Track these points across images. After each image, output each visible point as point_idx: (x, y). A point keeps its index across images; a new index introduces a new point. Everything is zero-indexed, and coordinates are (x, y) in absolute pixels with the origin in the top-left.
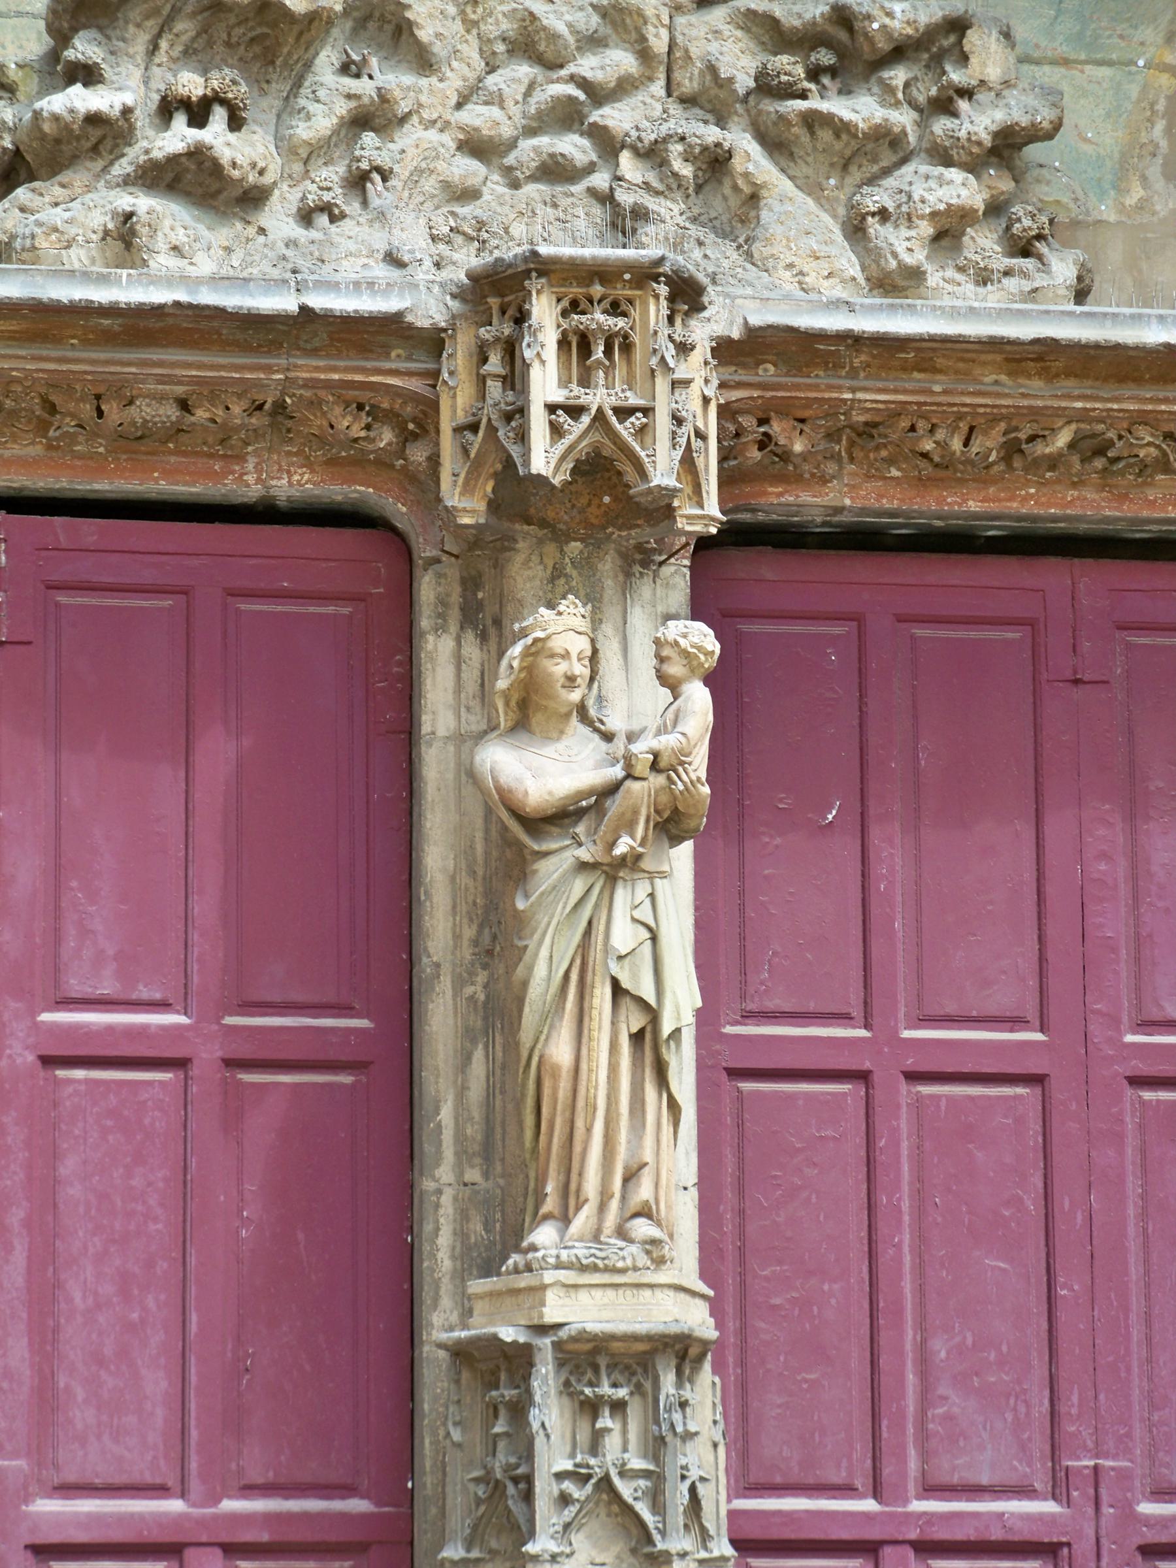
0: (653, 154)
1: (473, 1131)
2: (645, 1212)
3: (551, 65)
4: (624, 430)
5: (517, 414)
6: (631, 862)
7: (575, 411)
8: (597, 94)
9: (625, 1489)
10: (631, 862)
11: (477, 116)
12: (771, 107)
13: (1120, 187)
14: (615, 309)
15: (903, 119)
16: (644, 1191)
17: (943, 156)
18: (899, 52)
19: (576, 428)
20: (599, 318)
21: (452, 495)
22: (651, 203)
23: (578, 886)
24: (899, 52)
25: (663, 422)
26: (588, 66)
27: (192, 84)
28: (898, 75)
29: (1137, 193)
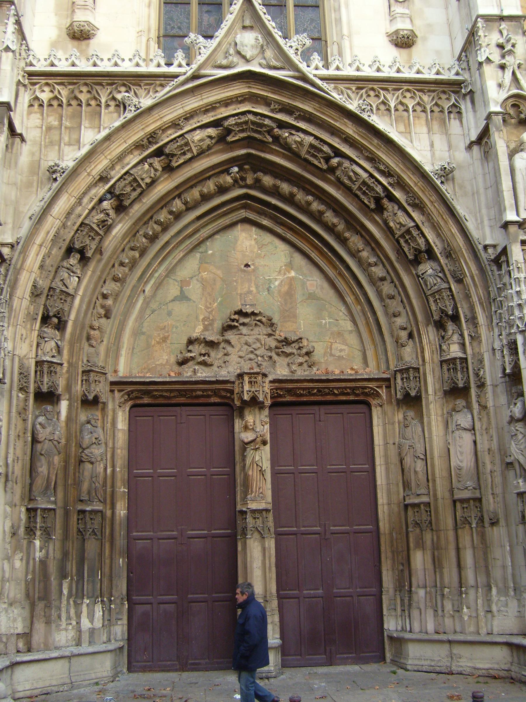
0: (262, 357)
1: (242, 483)
2: (262, 493)
3: (250, 346)
4: (256, 393)
5: (243, 392)
6: (258, 448)
7: (250, 391)
8: (255, 350)
9: (259, 529)
10: (258, 448)
11: (241, 354)
12: (277, 350)
13: (324, 357)
14: (255, 378)
15: (295, 351)
16: (261, 490)
17: (299, 355)
18: (293, 342)
19: (250, 393)
20: (253, 379)
21: (236, 402)
22: (262, 363)
23: (252, 452)
24: (293, 342)
25: (261, 392)
26: (254, 346)
27: (203, 352)
28: (293, 345)
29: (326, 358)
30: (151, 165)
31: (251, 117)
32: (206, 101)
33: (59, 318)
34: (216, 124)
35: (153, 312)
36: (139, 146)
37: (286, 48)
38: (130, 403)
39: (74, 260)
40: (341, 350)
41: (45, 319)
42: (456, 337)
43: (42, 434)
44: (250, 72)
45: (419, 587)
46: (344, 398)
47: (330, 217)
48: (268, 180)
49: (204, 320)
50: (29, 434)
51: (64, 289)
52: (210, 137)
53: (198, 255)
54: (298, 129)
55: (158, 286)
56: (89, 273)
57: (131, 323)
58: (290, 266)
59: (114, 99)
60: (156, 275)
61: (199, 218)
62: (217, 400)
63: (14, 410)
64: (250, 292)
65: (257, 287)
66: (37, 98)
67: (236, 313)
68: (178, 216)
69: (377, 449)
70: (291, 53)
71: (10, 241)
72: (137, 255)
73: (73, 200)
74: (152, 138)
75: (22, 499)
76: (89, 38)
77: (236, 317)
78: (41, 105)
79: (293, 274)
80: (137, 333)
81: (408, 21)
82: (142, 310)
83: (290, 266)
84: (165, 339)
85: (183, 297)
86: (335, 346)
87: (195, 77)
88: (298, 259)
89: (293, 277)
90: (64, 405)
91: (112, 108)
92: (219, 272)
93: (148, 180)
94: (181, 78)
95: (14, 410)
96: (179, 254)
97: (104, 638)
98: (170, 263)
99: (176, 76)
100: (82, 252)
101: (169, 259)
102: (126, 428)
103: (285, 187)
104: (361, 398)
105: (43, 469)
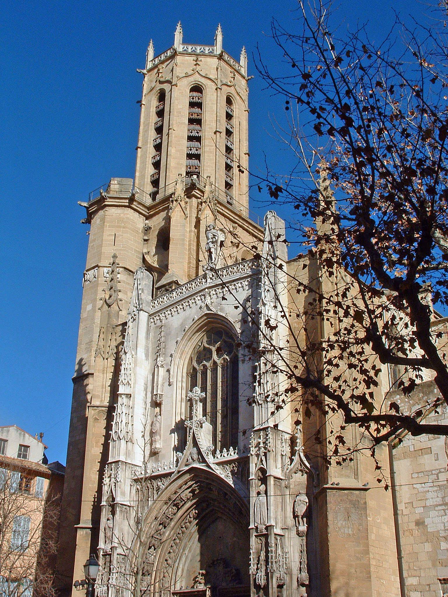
32: (185, 480)
36: (166, 503)
39: (152, 550)
66: (138, 489)
74: (170, 499)
76: (158, 453)
87: (179, 472)
100: (154, 546)
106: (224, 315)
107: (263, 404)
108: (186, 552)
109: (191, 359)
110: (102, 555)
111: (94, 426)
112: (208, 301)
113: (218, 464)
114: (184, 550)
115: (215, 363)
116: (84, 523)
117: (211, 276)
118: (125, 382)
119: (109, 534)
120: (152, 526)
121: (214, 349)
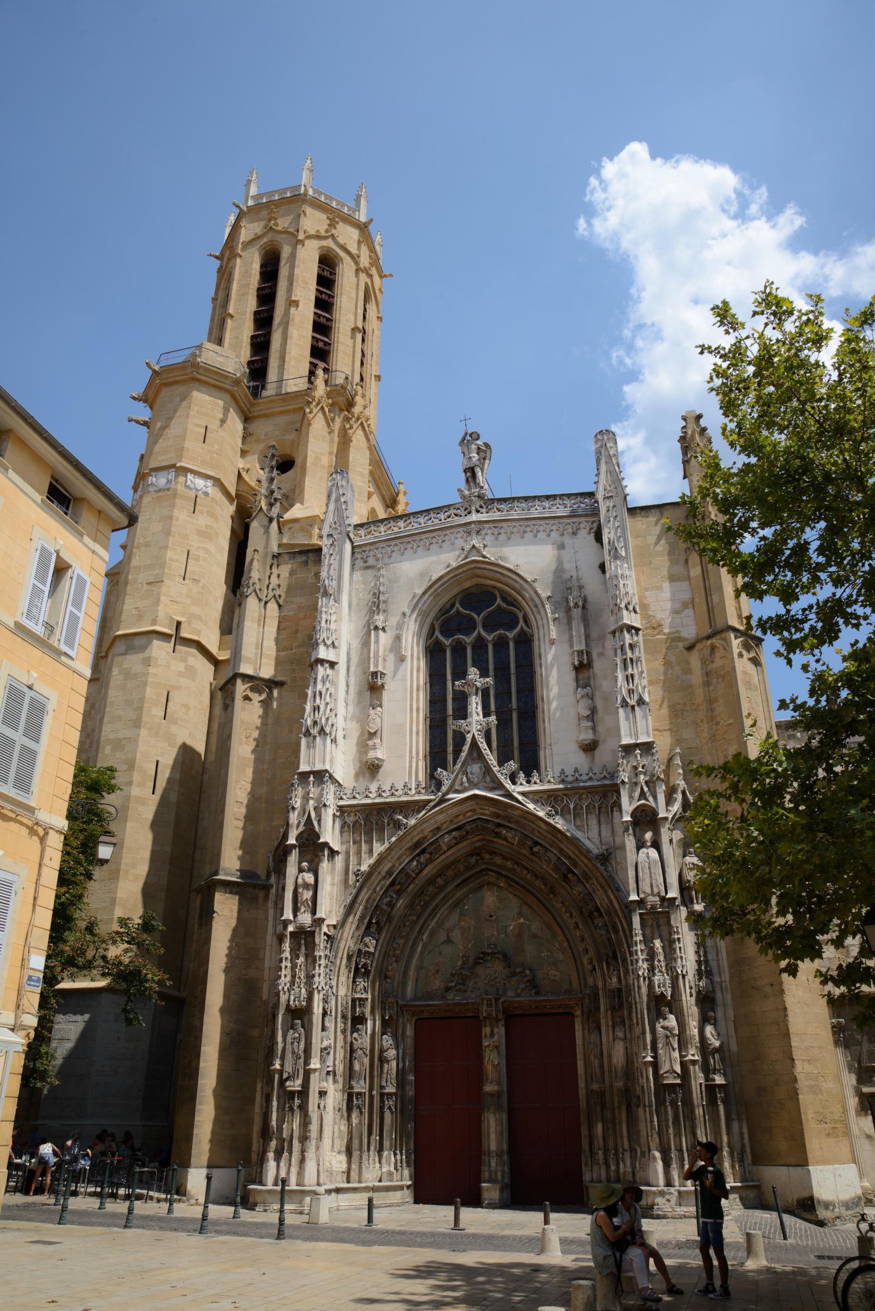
30: (418, 861)
31: (479, 823)
33: (365, 969)
34: (459, 828)
35: (430, 952)
37: (499, 775)
38: (415, 1018)
40: (555, 976)
41: (357, 970)
42: (615, 973)
43: (356, 1045)
44: (475, 795)
45: (599, 1149)
46: (555, 1011)
47: (538, 883)
48: (498, 860)
49: (463, 956)
50: (349, 1045)
51: (367, 949)
52: (455, 838)
53: (458, 910)
54: (512, 828)
55: (433, 933)
56: (384, 934)
57: (414, 961)
58: (520, 914)
59: (392, 819)
60: (430, 927)
61: (456, 886)
62: (471, 1015)
63: (339, 1030)
64: (493, 935)
65: (498, 931)
67: (482, 953)
68: (442, 888)
69: (578, 1048)
70: (502, 778)
71: (334, 923)
72: (415, 918)
73: (370, 892)
74: (417, 844)
75: (344, 1086)
77: (481, 956)
78: (349, 827)
79: (522, 920)
80: (419, 968)
81: (590, 731)
82: (422, 952)
83: (520, 914)
84: (437, 972)
85: (449, 941)
86: (551, 972)
87: (442, 801)
88: (525, 909)
89: (522, 923)
90: (369, 1023)
91: (391, 826)
92: (472, 922)
93: (417, 871)
94: (432, 804)
95: (339, 1030)
96: (443, 910)
97: (399, 1177)
98: (439, 919)
99: (430, 801)
101: (438, 915)
102: (412, 1034)
103: (509, 864)
104: (568, 1010)
105: (357, 1067)
106: (512, 567)
107: (637, 708)
108: (425, 937)
109: (432, 629)
110: (291, 933)
111: (243, 709)
112: (476, 541)
113: (523, 794)
114: (421, 932)
115: (480, 638)
116: (227, 874)
117: (478, 507)
118: (329, 642)
119: (307, 895)
120: (378, 889)
121: (479, 619)
